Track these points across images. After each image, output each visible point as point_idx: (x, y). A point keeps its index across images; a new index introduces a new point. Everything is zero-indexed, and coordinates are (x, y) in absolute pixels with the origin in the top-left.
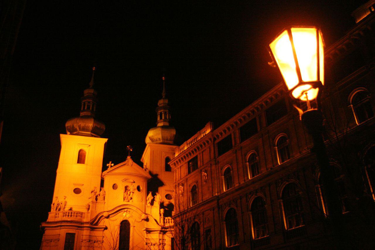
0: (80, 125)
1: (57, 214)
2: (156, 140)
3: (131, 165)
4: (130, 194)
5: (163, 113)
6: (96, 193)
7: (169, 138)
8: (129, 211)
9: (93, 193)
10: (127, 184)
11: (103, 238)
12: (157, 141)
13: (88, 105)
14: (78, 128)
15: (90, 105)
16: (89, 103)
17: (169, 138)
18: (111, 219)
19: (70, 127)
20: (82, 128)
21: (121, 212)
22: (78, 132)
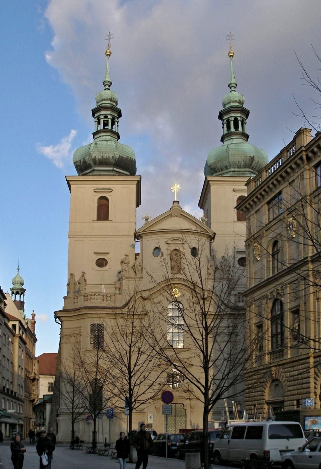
0: (95, 157)
2: (220, 168)
5: (230, 119)
6: (128, 264)
7: (242, 165)
9: (124, 265)
10: (173, 247)
12: (222, 170)
13: (103, 121)
14: (92, 163)
15: (108, 121)
16: (106, 117)
17: (242, 165)
19: (80, 163)
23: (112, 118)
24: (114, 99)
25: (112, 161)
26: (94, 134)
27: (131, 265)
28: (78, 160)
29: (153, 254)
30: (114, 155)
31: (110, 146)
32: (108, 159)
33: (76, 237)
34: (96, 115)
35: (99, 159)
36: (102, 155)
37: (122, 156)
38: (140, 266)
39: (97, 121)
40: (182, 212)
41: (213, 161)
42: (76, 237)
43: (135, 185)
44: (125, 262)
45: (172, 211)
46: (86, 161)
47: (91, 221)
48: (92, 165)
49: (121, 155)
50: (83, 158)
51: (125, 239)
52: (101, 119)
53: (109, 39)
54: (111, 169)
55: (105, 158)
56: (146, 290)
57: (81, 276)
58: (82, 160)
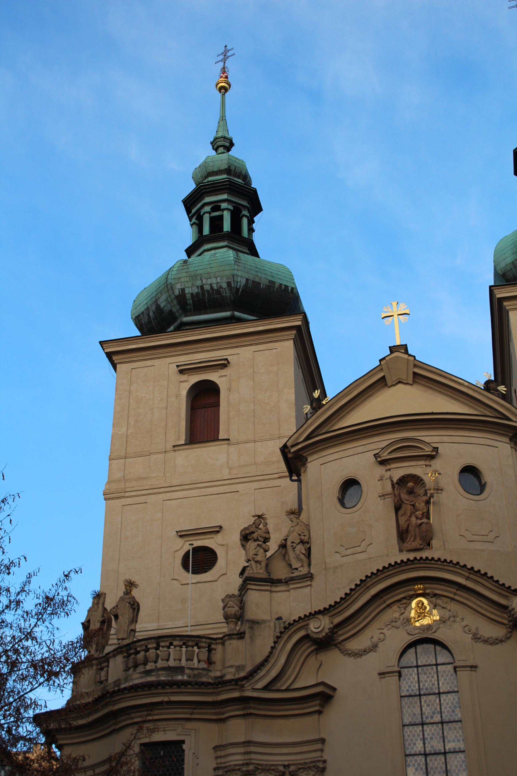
0: (183, 290)
1: (102, 669)
3: (411, 383)
4: (428, 512)
6: (266, 540)
8: (435, 595)
9: (252, 545)
11: (322, 750)
13: (212, 219)
14: (176, 308)
15: (221, 217)
16: (216, 207)
18: (354, 645)
19: (148, 315)
20: (190, 302)
21: (395, 607)
22: (176, 324)
23: (232, 208)
24: (238, 170)
25: (227, 293)
26: (190, 251)
27: (273, 546)
28: (143, 309)
29: (342, 501)
30: (231, 280)
31: (220, 260)
32: (218, 291)
33: (127, 494)
34: (194, 211)
35: (192, 294)
36: (199, 283)
37: (254, 282)
38: (302, 542)
39: (196, 221)
40: (415, 366)
41: (509, 260)
42: (127, 494)
43: (292, 341)
44: (255, 535)
45: (384, 368)
46: (162, 305)
47: (169, 447)
48: (177, 314)
49: (251, 277)
50: (154, 300)
51: (263, 484)
52: (204, 214)
53: (224, 60)
54: (228, 314)
55: (208, 291)
56: (319, 612)
57: (122, 595)
58: (154, 308)
